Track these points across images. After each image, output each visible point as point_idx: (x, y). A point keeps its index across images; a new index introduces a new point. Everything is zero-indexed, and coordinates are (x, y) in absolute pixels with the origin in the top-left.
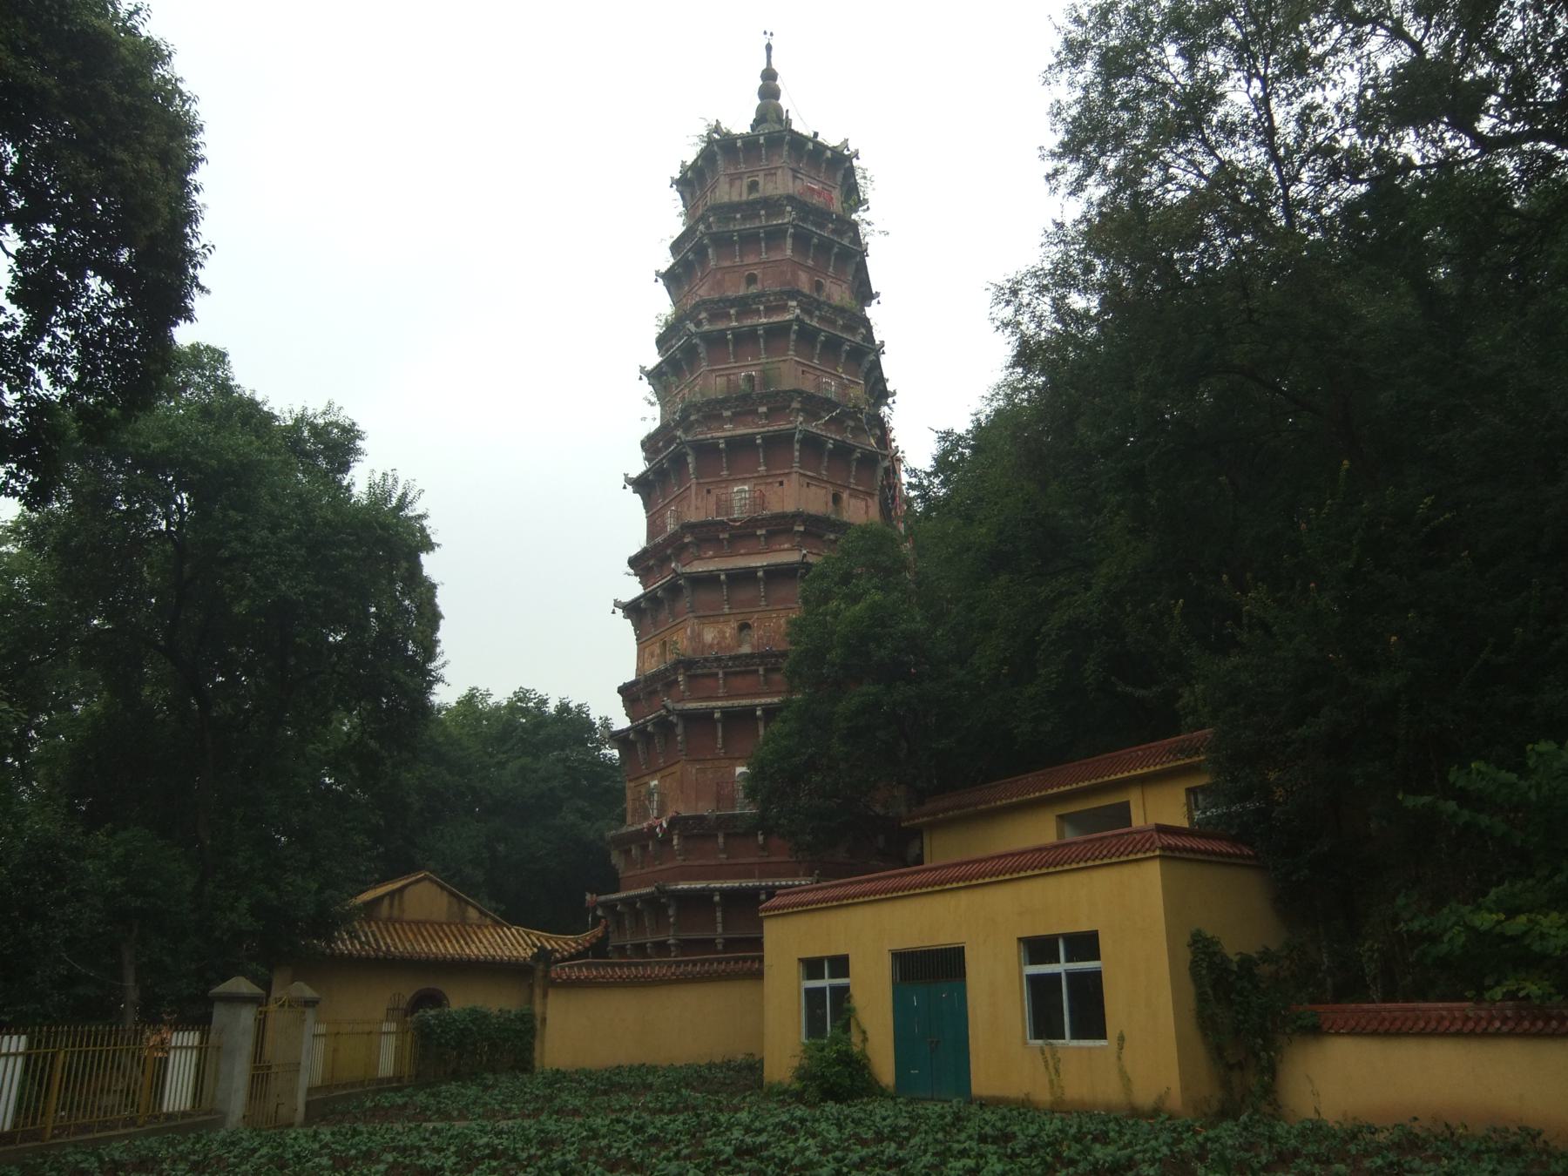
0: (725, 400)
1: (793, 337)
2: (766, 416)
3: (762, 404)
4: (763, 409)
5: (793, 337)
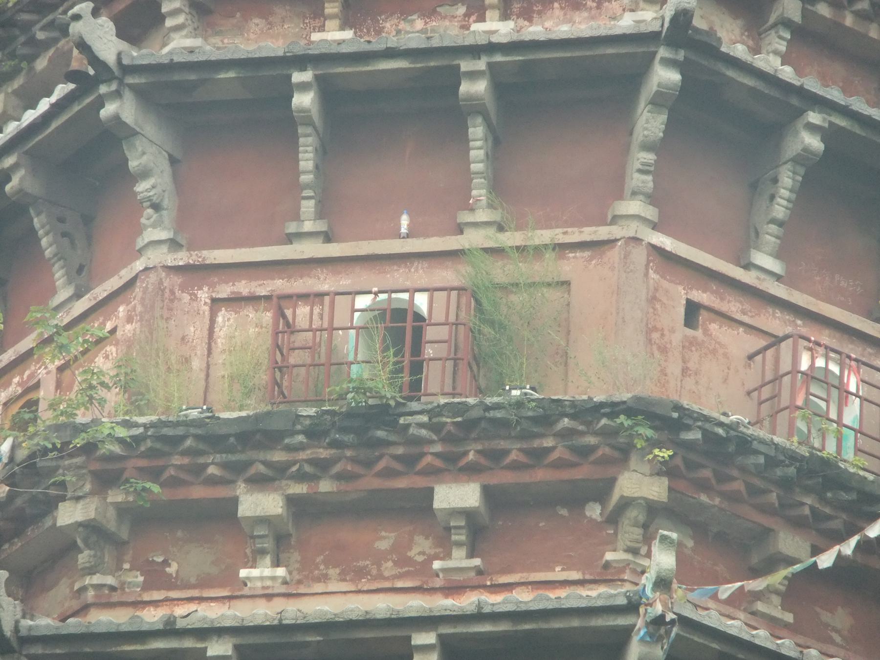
0: (254, 435)
1: (650, 123)
2: (477, 530)
3: (454, 467)
4: (458, 495)
5: (650, 123)
